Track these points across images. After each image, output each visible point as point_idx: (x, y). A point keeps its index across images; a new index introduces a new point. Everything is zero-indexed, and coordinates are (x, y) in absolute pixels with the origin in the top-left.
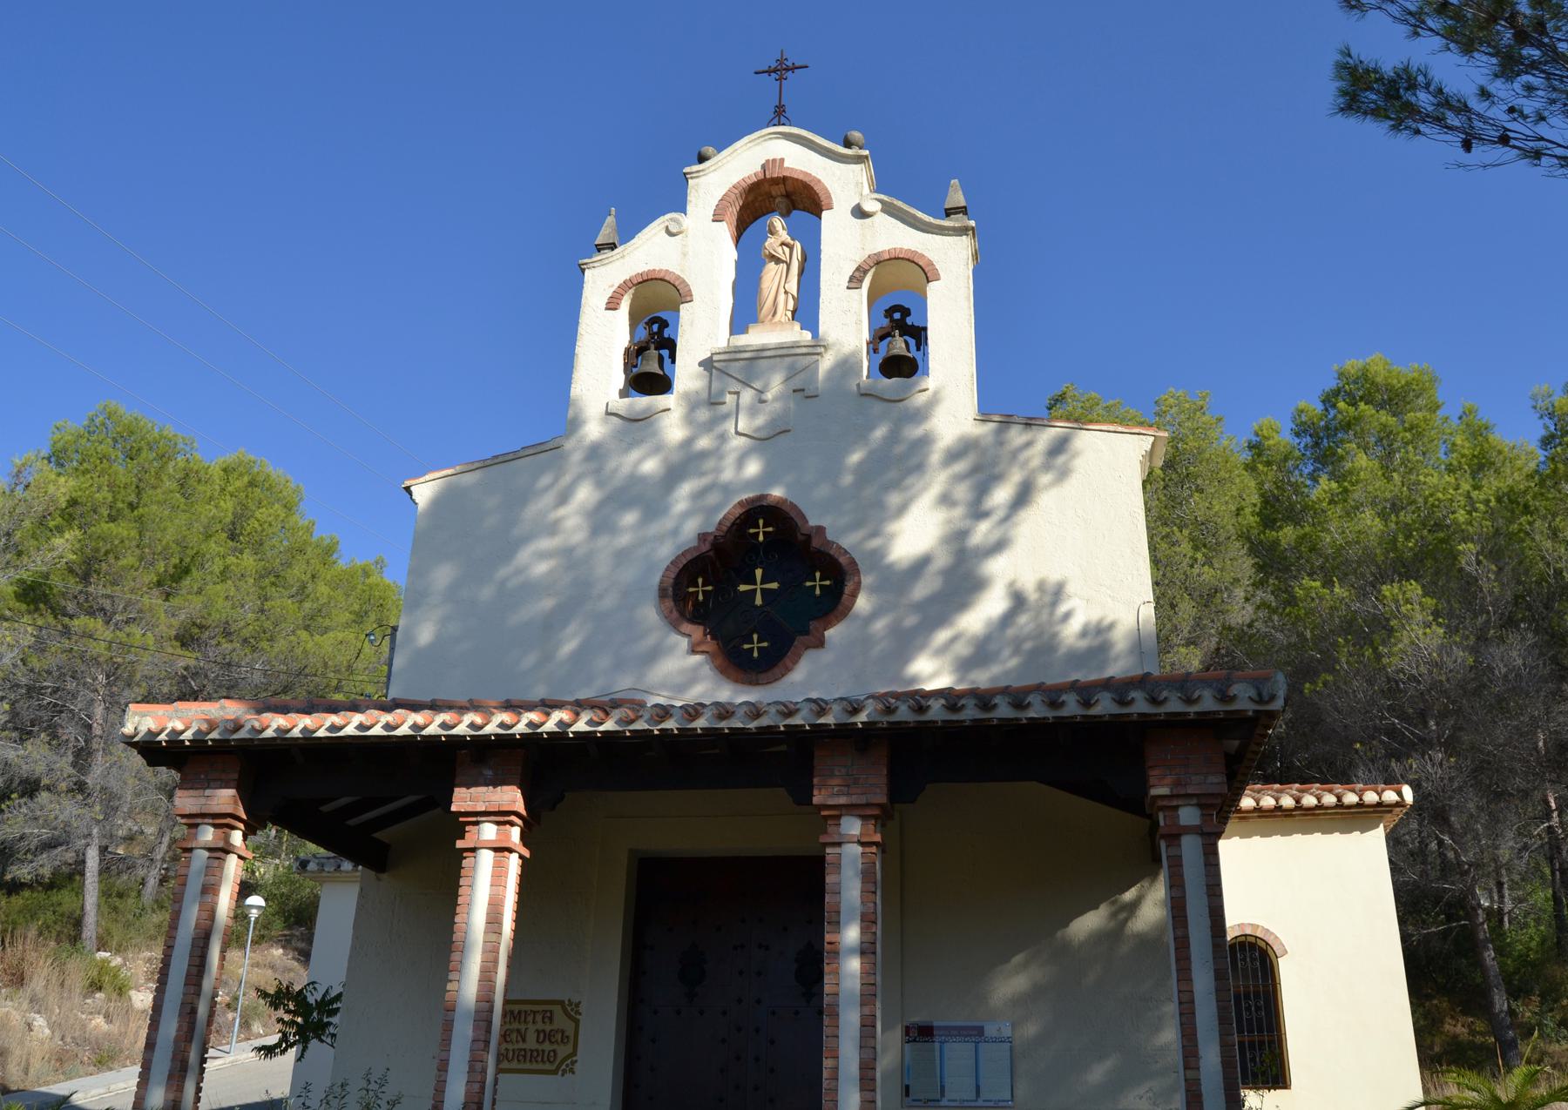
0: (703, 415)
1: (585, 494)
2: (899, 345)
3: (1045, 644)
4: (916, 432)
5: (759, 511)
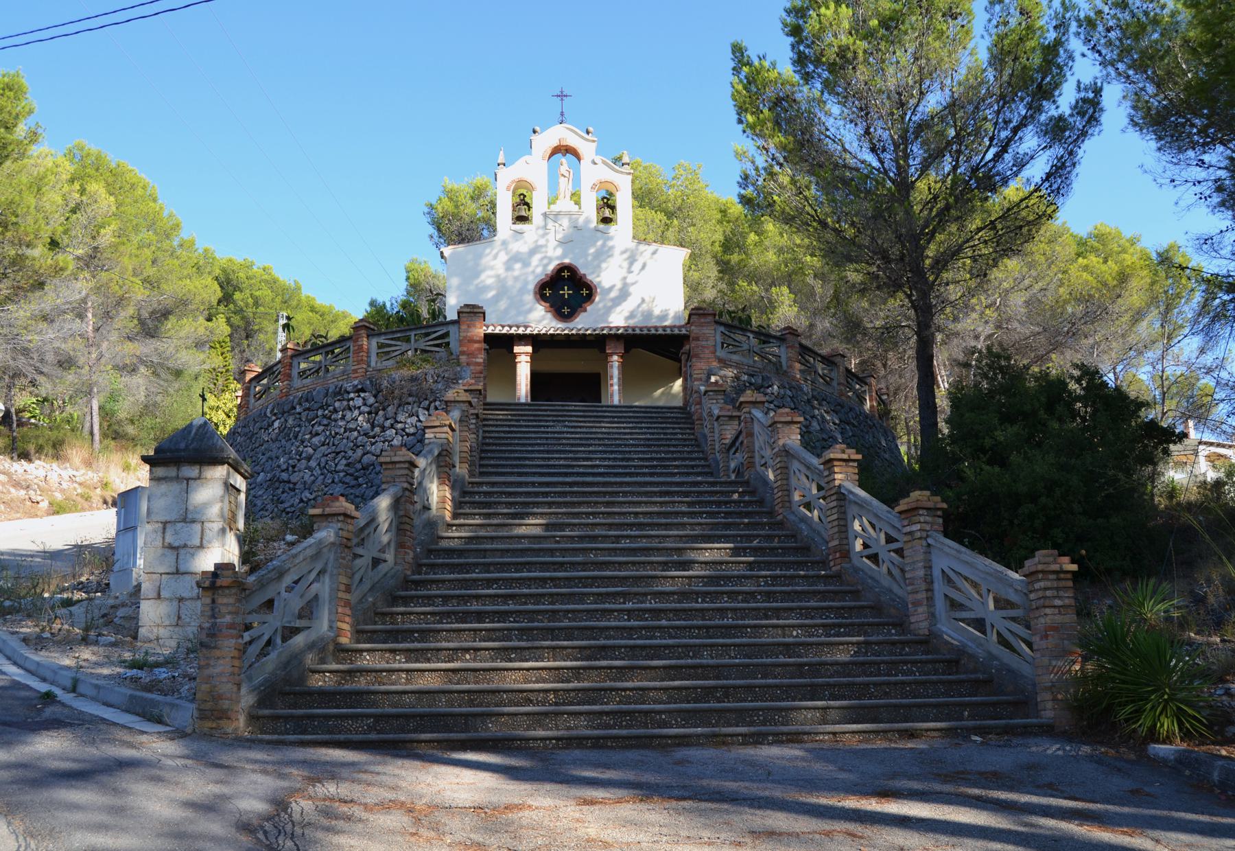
0: (541, 232)
1: (503, 257)
2: (607, 213)
3: (649, 314)
4: (610, 243)
5: (562, 268)
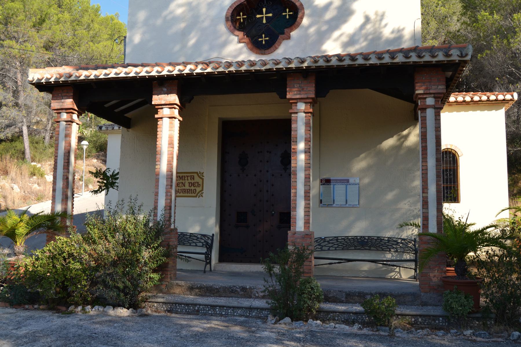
3: (377, 37)
